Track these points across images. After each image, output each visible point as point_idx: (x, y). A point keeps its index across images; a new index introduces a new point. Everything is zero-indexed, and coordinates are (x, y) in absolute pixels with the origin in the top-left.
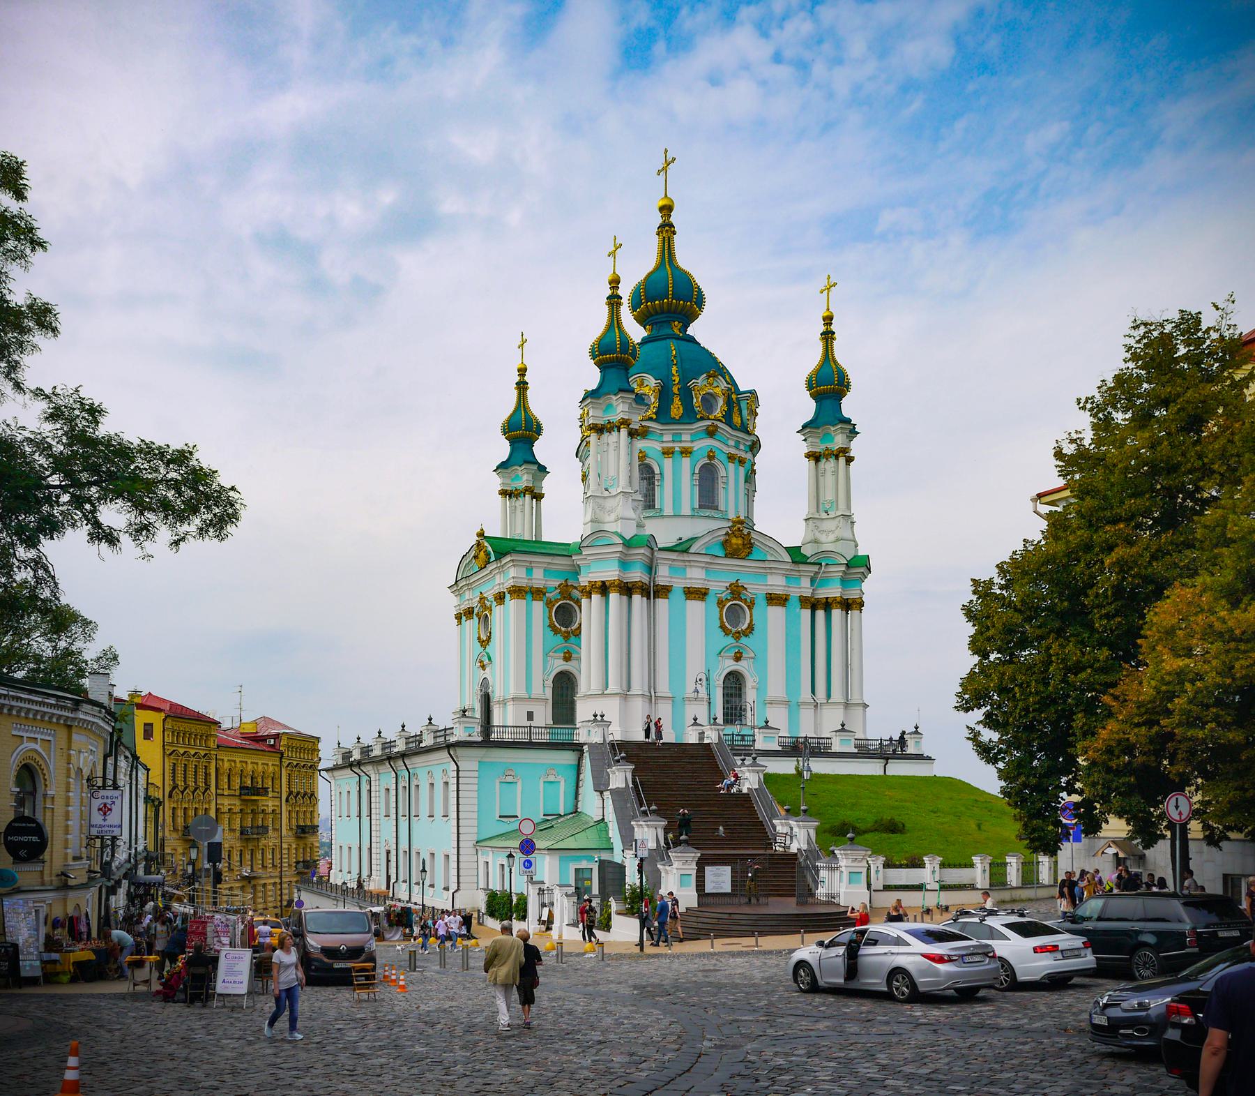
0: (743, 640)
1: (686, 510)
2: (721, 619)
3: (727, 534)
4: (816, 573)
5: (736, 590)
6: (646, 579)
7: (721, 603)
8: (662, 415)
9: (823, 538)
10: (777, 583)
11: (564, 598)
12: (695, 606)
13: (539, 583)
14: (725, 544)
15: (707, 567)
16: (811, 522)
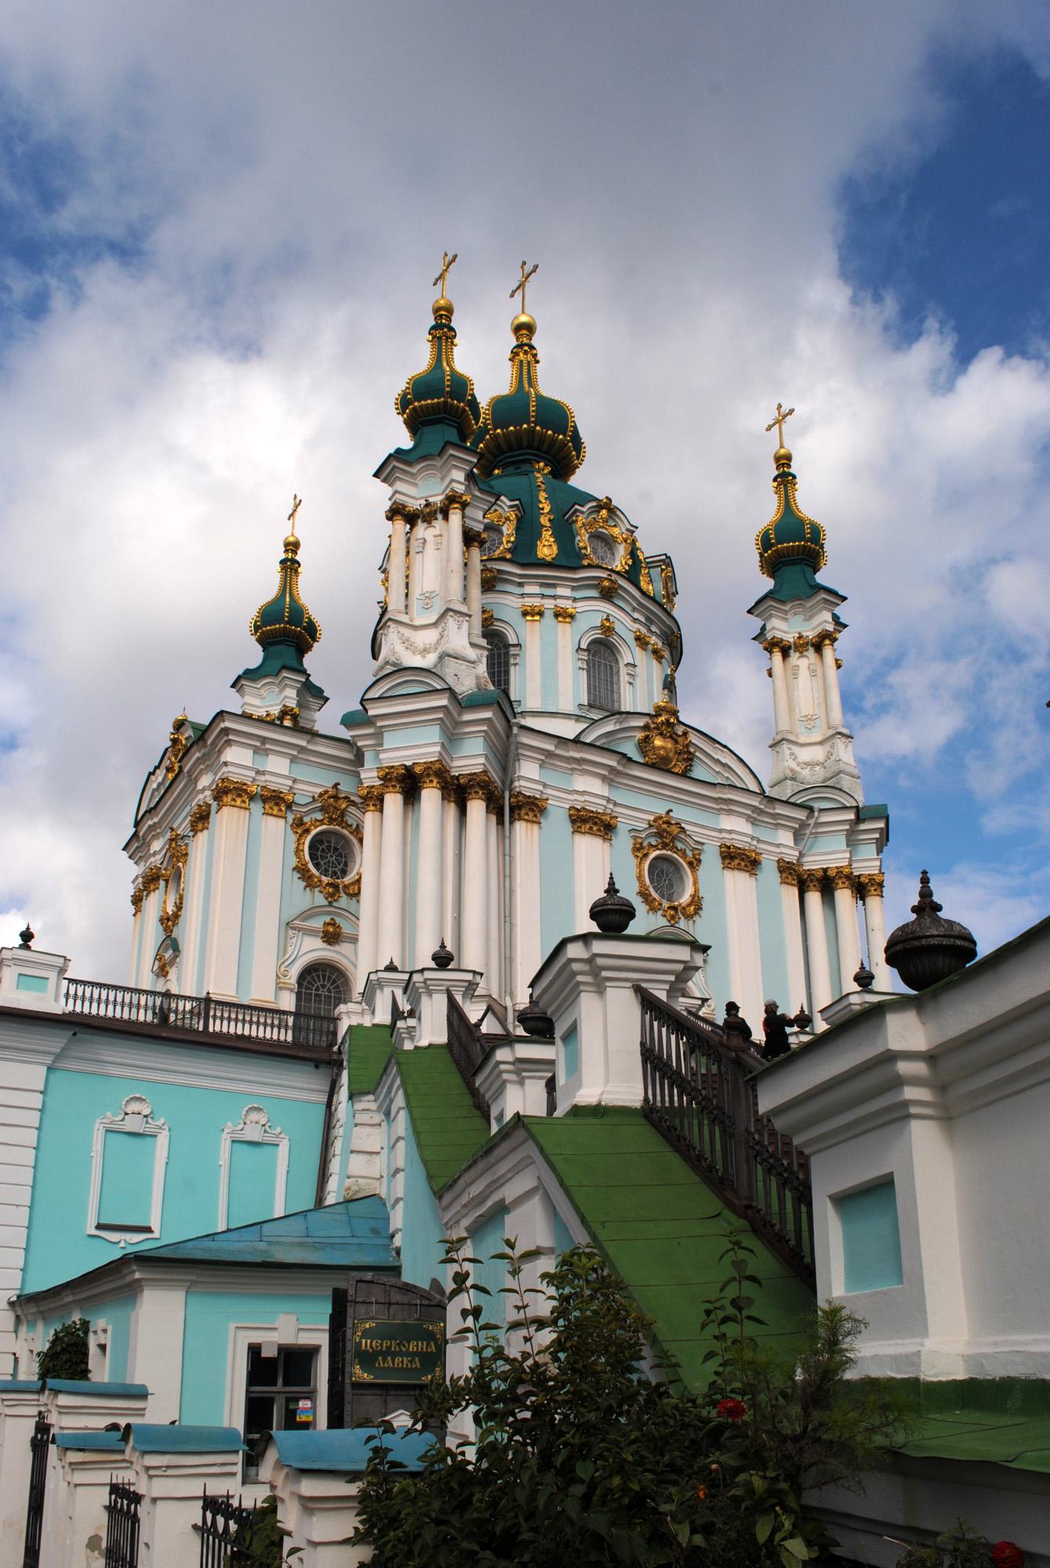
0: (682, 923)
1: (568, 705)
2: (640, 878)
3: (646, 727)
4: (803, 825)
5: (666, 832)
6: (495, 776)
7: (639, 849)
8: (523, 554)
9: (805, 773)
10: (737, 828)
11: (331, 821)
12: (588, 846)
13: (281, 784)
14: (644, 745)
15: (611, 777)
16: (785, 745)
